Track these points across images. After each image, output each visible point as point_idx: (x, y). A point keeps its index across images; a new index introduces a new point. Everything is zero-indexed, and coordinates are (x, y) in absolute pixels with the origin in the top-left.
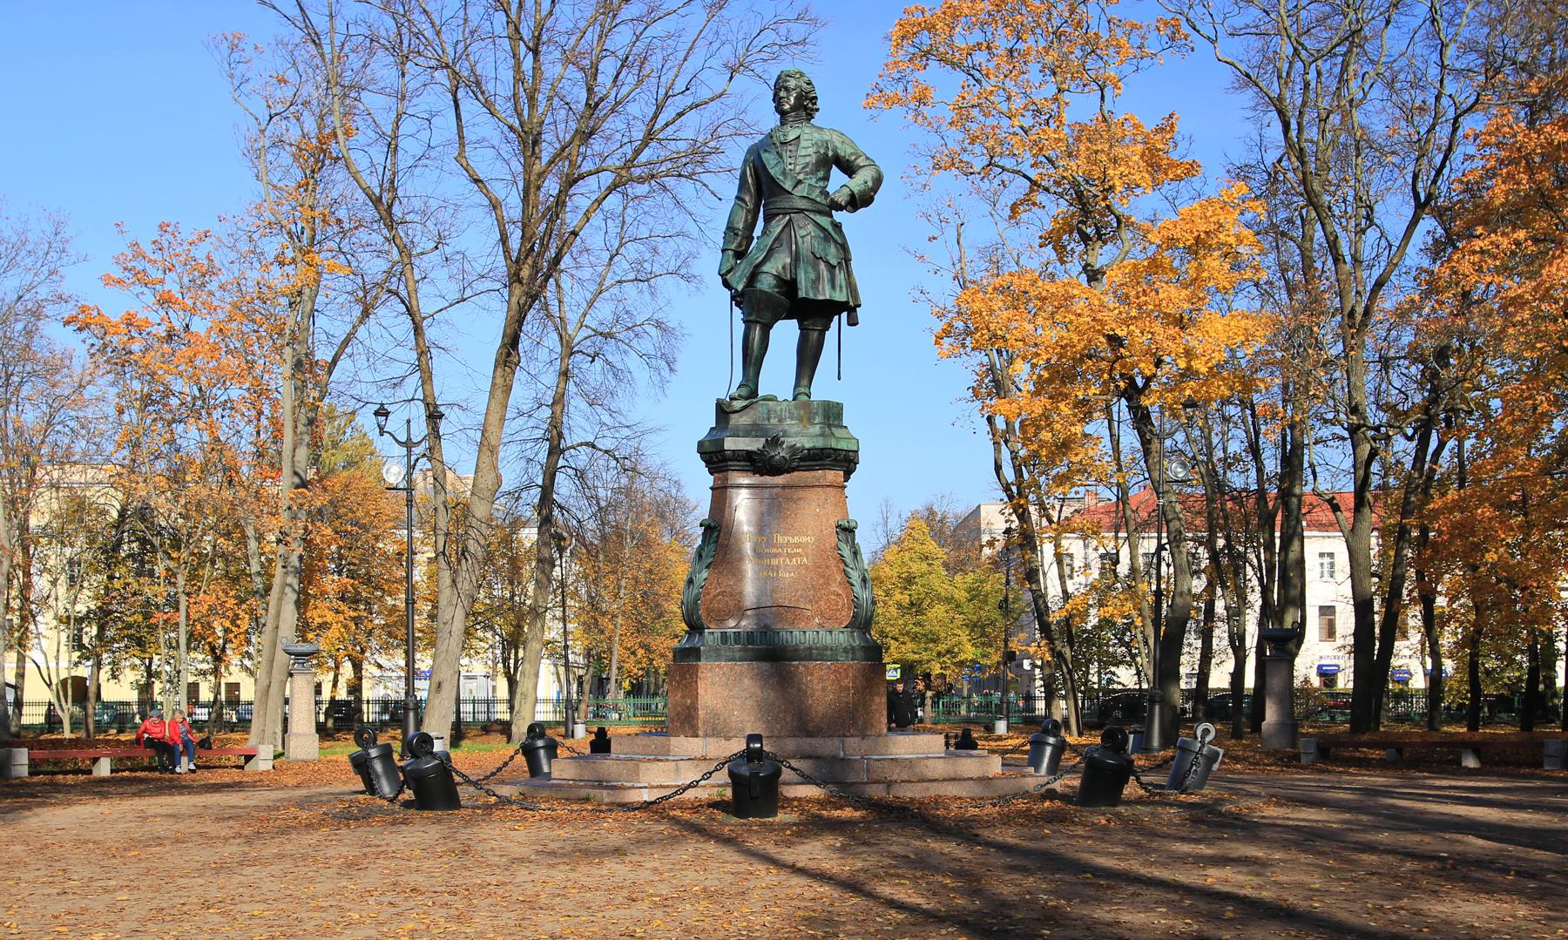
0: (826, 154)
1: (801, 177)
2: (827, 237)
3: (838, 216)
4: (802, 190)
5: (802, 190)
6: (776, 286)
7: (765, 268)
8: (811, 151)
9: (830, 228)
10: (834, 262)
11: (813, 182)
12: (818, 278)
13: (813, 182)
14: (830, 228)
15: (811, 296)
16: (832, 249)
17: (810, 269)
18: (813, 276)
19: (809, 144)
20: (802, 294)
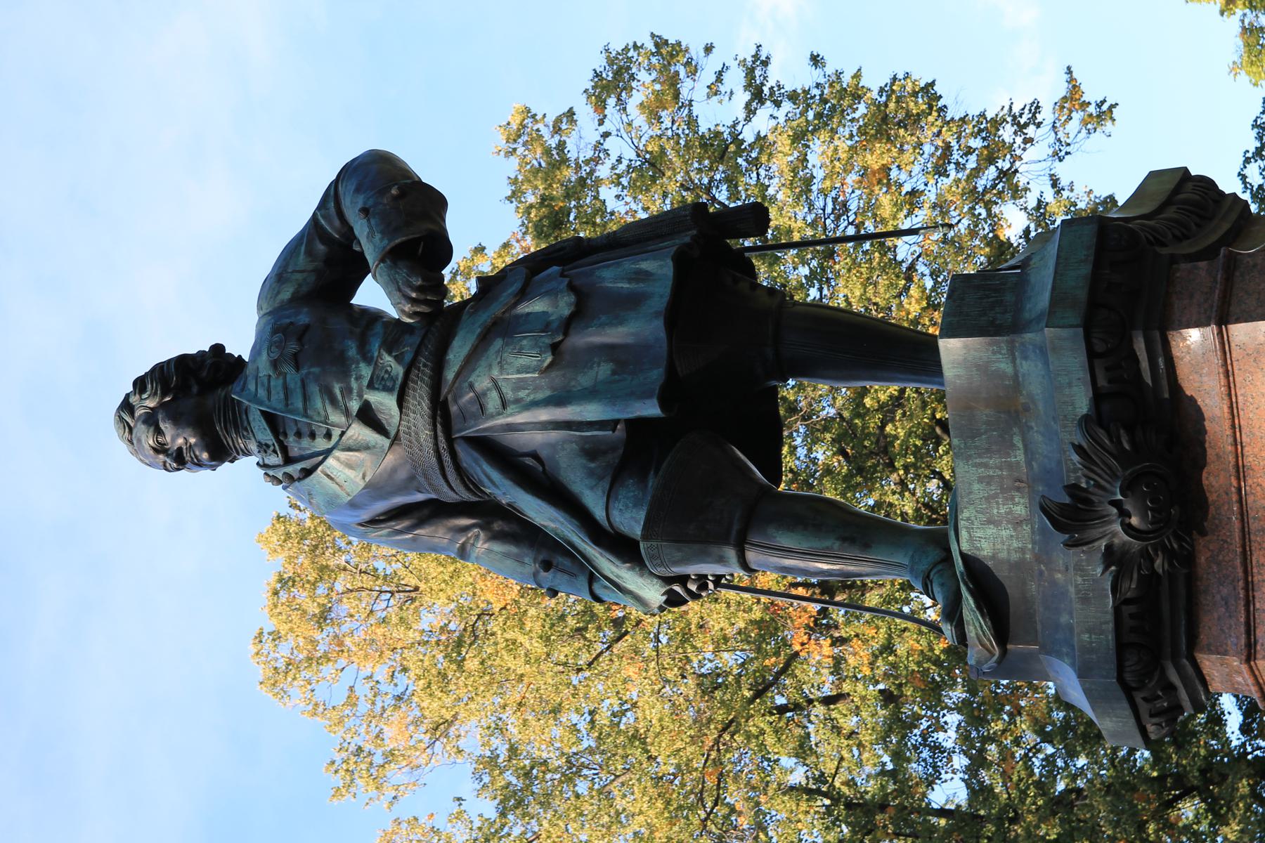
0: (301, 334)
1: (355, 406)
2: (503, 329)
3: (461, 289)
4: (385, 403)
5: (385, 403)
6: (643, 479)
7: (599, 513)
8: (293, 377)
9: (485, 317)
10: (564, 306)
11: (366, 371)
12: (609, 351)
13: (366, 371)
14: (485, 317)
15: (656, 375)
16: (537, 306)
17: (584, 380)
18: (604, 370)
19: (277, 384)
20: (651, 409)
